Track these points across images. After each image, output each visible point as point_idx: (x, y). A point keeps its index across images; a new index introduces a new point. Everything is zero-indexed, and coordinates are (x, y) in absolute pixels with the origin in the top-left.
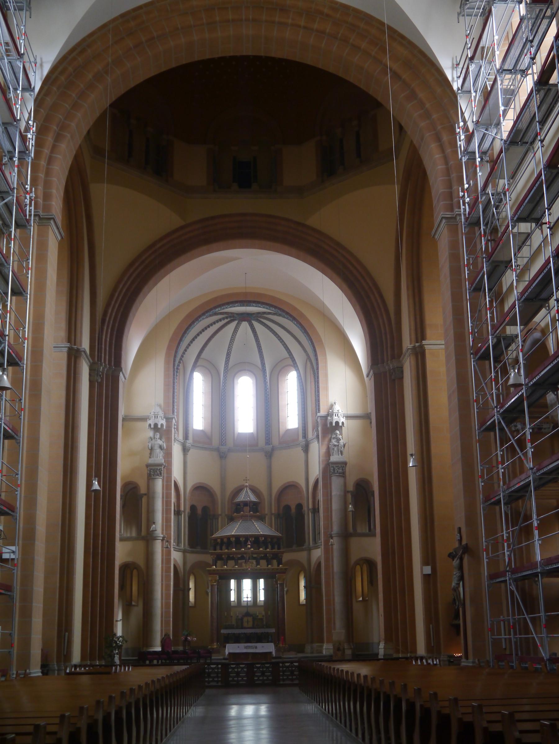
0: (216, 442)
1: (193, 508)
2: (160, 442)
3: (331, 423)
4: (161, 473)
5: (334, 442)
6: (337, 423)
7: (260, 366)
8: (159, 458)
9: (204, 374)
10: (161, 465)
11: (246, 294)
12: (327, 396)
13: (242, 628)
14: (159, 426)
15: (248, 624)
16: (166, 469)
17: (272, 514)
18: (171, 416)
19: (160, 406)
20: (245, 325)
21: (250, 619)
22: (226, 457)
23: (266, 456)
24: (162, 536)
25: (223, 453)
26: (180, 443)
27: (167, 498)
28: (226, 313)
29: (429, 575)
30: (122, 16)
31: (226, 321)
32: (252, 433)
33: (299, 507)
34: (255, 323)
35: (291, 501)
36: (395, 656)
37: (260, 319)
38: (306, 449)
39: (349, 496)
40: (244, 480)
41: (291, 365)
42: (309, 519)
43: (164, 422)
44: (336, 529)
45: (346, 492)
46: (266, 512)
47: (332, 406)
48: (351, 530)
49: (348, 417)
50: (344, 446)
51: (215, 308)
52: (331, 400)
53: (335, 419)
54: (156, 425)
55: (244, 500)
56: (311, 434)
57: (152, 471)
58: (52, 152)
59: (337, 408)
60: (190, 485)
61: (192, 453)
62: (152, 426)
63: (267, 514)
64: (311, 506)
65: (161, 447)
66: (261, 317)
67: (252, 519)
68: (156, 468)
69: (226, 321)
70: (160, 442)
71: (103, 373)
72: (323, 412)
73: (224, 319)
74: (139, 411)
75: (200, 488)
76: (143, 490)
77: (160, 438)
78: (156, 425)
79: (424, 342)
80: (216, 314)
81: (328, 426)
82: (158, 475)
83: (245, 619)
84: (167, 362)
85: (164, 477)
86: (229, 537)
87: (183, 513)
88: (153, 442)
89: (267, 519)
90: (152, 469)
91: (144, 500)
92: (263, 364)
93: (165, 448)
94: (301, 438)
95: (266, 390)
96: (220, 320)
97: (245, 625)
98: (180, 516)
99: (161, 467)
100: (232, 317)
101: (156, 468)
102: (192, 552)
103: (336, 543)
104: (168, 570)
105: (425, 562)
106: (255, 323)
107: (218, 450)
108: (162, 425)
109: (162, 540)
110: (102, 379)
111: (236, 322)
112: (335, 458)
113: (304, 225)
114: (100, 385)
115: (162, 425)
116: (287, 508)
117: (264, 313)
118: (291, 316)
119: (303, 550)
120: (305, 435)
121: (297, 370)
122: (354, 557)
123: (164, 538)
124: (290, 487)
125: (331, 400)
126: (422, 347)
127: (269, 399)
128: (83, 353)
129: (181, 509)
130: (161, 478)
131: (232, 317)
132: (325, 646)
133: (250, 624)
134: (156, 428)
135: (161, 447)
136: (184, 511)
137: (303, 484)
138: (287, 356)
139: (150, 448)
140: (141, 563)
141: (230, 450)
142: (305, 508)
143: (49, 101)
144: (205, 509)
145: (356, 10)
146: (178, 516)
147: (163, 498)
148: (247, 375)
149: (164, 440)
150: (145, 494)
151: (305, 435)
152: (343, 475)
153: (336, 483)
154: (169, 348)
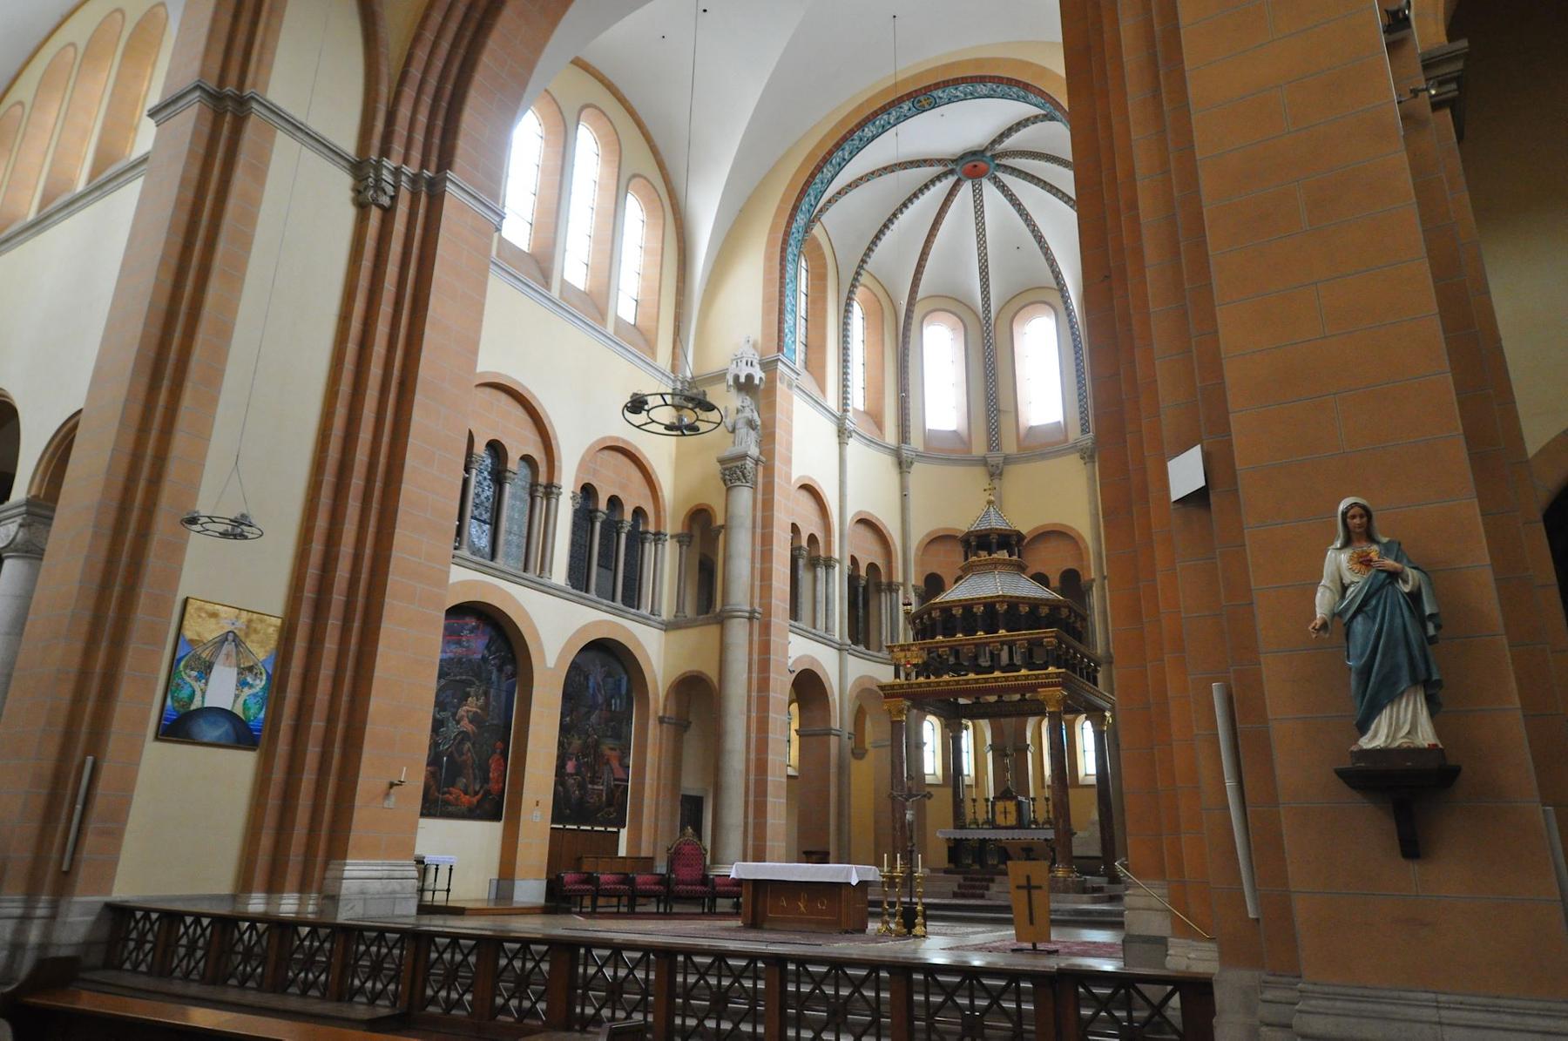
0: (979, 449)
2: (747, 413)
4: (745, 477)
7: (1055, 286)
8: (750, 445)
10: (744, 456)
13: (993, 824)
14: (742, 380)
15: (1006, 817)
16: (764, 467)
17: (1105, 578)
18: (773, 354)
19: (755, 346)
21: (1011, 806)
22: (1001, 474)
23: (1082, 458)
24: (748, 608)
25: (992, 466)
26: (889, 451)
27: (764, 527)
32: (1059, 422)
34: (1000, 175)
37: (1004, 161)
40: (985, 490)
46: (1093, 577)
54: (737, 378)
55: (978, 528)
57: (727, 472)
60: (918, 536)
61: (917, 468)
62: (731, 382)
63: (1093, 580)
65: (751, 424)
67: (995, 568)
68: (735, 464)
71: (396, 187)
74: (715, 364)
76: (720, 521)
78: (737, 378)
82: (739, 479)
84: (768, 258)
85: (755, 483)
87: (901, 588)
88: (740, 415)
89: (1094, 589)
90: (725, 469)
91: (721, 537)
92: (1057, 275)
93: (759, 423)
95: (1072, 327)
98: (894, 595)
99: (743, 462)
101: (735, 464)
104: (764, 684)
107: (984, 462)
108: (749, 377)
109: (751, 619)
110: (394, 199)
114: (388, 213)
115: (749, 377)
118: (1017, 83)
123: (752, 612)
127: (1080, 342)
128: (255, 105)
129: (894, 580)
130: (748, 484)
133: (1012, 819)
134: (745, 386)
135: (751, 424)
136: (904, 584)
139: (730, 429)
140: (712, 673)
141: (1008, 460)
146: (891, 594)
147: (754, 527)
150: (722, 527)
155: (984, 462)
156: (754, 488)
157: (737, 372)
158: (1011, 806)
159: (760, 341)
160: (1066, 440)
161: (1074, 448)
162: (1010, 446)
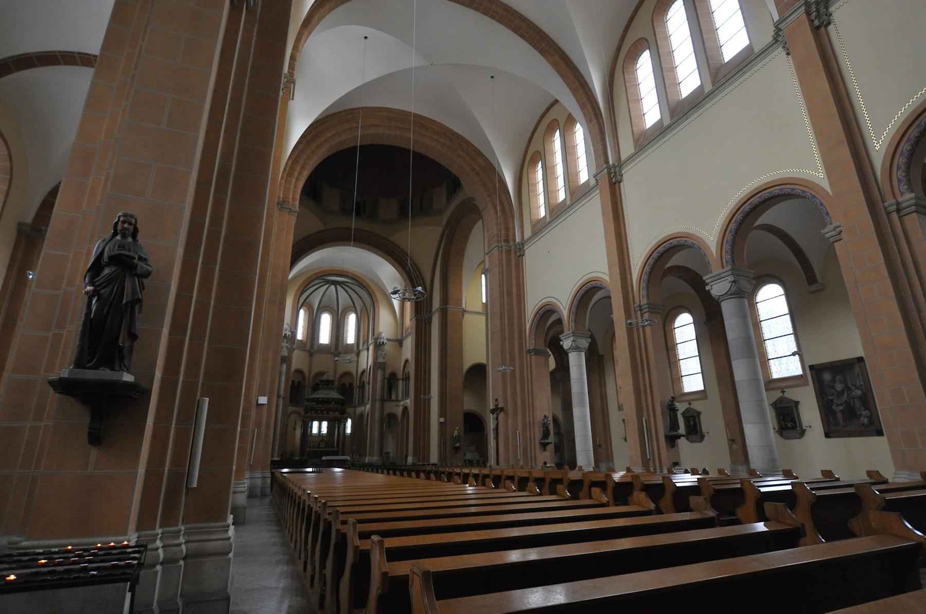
0: (308, 347)
1: (293, 381)
3: (380, 342)
5: (380, 352)
6: (383, 342)
9: (305, 311)
11: (342, 271)
12: (378, 328)
13: (319, 448)
14: (287, 336)
20: (333, 287)
21: (324, 443)
28: (326, 280)
29: (443, 422)
30: (345, 111)
31: (324, 283)
32: (328, 344)
33: (351, 385)
34: (338, 286)
35: (347, 381)
36: (418, 463)
38: (358, 355)
39: (386, 381)
41: (353, 311)
42: (356, 391)
43: (290, 333)
44: (378, 396)
45: (384, 378)
47: (381, 333)
48: (385, 398)
49: (388, 340)
50: (385, 354)
51: (323, 276)
52: (381, 330)
53: (382, 340)
56: (361, 348)
58: (299, 175)
59: (383, 335)
64: (358, 384)
66: (343, 284)
69: (324, 283)
70: (286, 344)
72: (375, 337)
73: (323, 282)
75: (299, 371)
77: (287, 342)
79: (448, 306)
80: (322, 279)
81: (378, 343)
83: (321, 443)
86: (318, 398)
94: (355, 348)
96: (321, 283)
97: (321, 446)
100: (335, 283)
102: (291, 406)
103: (378, 405)
105: (441, 415)
106: (339, 287)
107: (309, 351)
111: (328, 285)
112: (381, 360)
113: (388, 240)
115: (289, 335)
116: (344, 385)
117: (346, 282)
119: (351, 407)
120: (358, 347)
121: (356, 313)
122: (386, 411)
124: (347, 374)
125: (381, 330)
126: (446, 308)
131: (327, 282)
132: (367, 458)
133: (324, 446)
135: (287, 347)
137: (354, 373)
138: (352, 305)
142: (355, 385)
143: (301, 147)
144: (299, 383)
145: (462, 137)
148: (349, 315)
149: (289, 343)
151: (358, 347)
152: (384, 370)
153: (380, 374)
154: (296, 294)
155: (309, 351)
156: (287, 365)
157: (285, 333)
158: (324, 443)
159: (289, 323)
160: (330, 350)
161: (332, 353)
162: (316, 349)
